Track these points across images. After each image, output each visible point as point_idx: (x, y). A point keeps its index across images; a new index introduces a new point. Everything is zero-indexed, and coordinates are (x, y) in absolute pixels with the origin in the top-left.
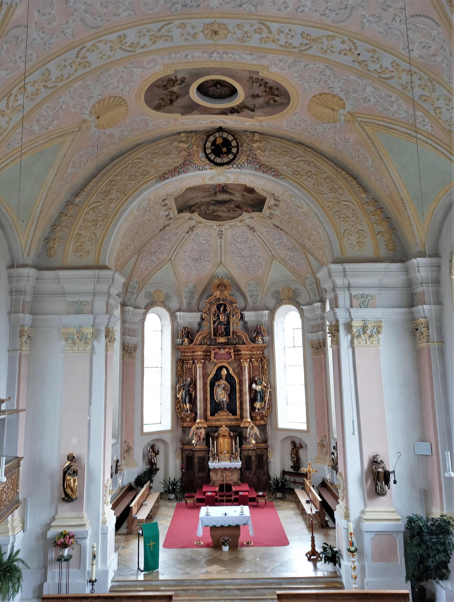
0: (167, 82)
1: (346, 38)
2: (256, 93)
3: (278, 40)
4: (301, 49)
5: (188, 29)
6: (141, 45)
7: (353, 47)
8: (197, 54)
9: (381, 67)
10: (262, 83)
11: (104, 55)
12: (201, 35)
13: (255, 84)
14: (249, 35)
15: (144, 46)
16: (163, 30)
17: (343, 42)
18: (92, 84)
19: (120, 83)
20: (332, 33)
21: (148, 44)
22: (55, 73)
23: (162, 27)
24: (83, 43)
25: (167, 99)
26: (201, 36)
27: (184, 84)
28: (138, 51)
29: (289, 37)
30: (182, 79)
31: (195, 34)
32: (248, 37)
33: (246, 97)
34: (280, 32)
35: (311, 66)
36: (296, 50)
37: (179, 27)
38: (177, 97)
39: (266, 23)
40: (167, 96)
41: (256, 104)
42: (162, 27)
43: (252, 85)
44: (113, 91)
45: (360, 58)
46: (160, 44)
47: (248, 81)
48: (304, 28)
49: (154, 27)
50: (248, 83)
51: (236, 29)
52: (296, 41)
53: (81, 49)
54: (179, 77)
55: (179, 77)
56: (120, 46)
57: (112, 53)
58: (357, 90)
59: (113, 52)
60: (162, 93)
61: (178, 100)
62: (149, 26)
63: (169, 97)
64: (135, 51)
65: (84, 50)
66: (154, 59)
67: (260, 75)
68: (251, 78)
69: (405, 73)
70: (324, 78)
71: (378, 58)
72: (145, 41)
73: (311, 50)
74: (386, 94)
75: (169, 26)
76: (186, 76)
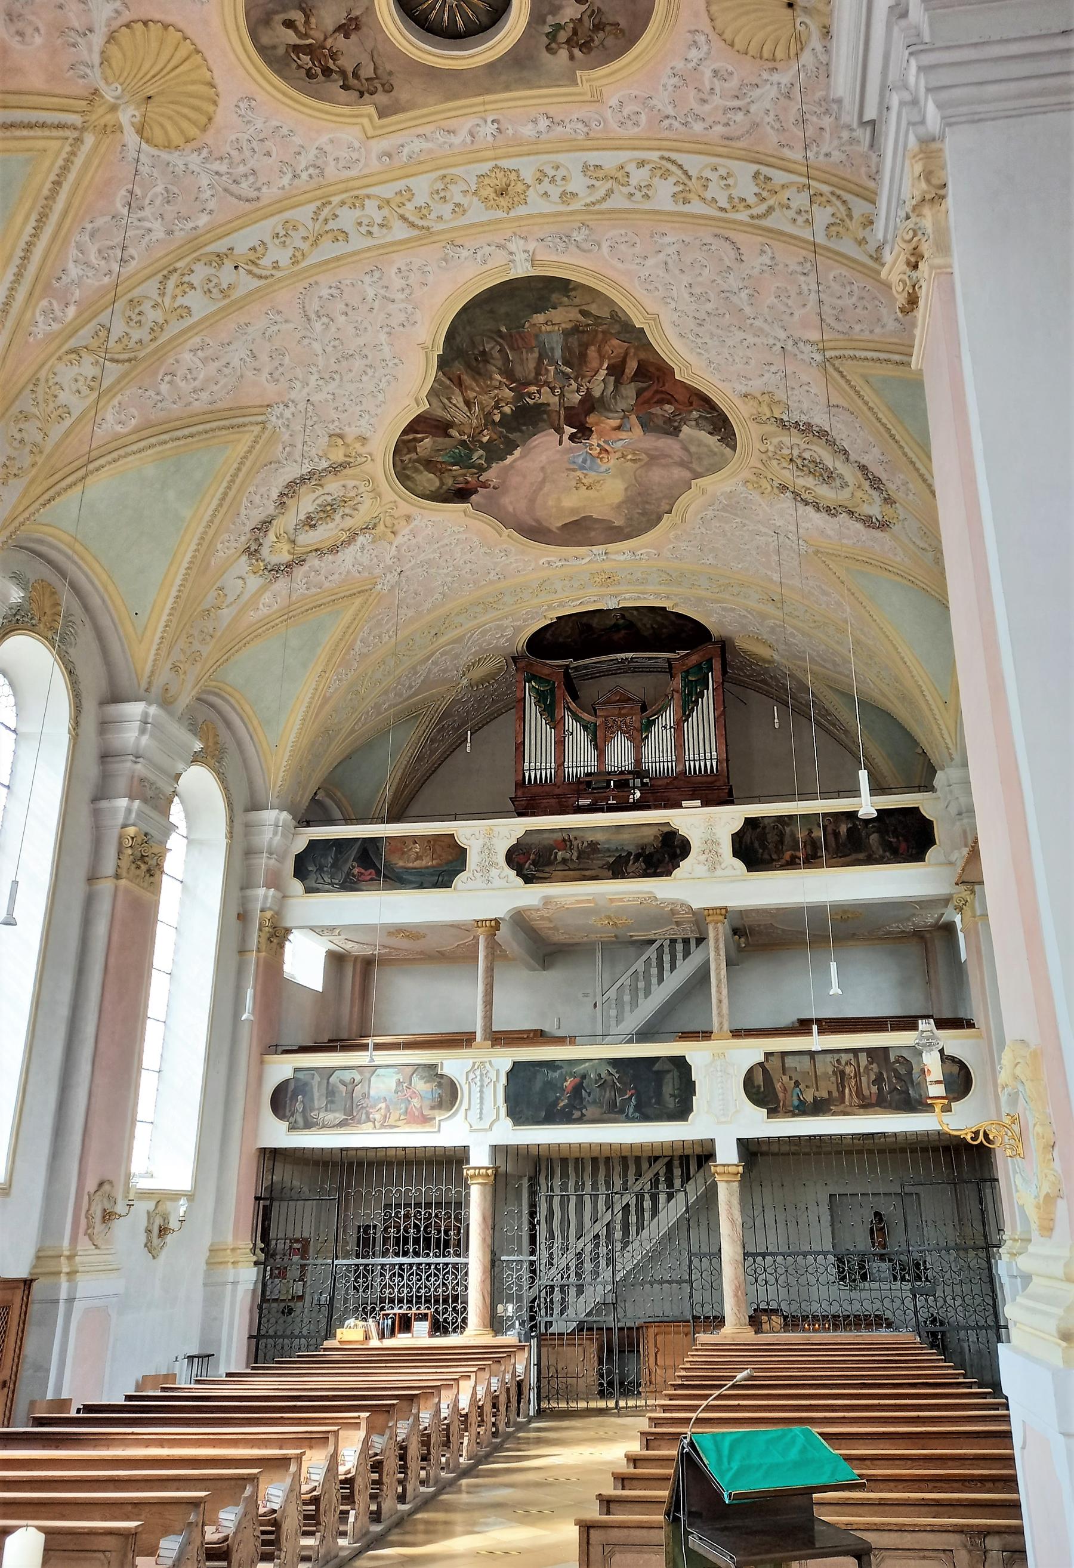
1: (278, 274)
3: (380, 208)
4: (329, 207)
5: (555, 191)
6: (648, 167)
8: (528, 131)
12: (529, 181)
14: (435, 196)
15: (641, 164)
16: (602, 192)
17: (276, 266)
20: (303, 264)
21: (634, 165)
23: (604, 199)
24: (751, 225)
26: (528, 175)
28: (654, 156)
29: (365, 222)
31: (540, 181)
32: (437, 192)
35: (286, 180)
36: (336, 200)
37: (574, 195)
39: (415, 232)
42: (604, 199)
45: (229, 265)
46: (609, 160)
47: (390, 73)
48: (349, 248)
49: (618, 202)
51: (464, 201)
52: (347, 218)
53: (759, 217)
54: (563, 53)
55: (563, 53)
57: (708, 173)
58: (168, 202)
64: (662, 158)
68: (389, 89)
69: (161, 321)
71: (210, 291)
72: (639, 176)
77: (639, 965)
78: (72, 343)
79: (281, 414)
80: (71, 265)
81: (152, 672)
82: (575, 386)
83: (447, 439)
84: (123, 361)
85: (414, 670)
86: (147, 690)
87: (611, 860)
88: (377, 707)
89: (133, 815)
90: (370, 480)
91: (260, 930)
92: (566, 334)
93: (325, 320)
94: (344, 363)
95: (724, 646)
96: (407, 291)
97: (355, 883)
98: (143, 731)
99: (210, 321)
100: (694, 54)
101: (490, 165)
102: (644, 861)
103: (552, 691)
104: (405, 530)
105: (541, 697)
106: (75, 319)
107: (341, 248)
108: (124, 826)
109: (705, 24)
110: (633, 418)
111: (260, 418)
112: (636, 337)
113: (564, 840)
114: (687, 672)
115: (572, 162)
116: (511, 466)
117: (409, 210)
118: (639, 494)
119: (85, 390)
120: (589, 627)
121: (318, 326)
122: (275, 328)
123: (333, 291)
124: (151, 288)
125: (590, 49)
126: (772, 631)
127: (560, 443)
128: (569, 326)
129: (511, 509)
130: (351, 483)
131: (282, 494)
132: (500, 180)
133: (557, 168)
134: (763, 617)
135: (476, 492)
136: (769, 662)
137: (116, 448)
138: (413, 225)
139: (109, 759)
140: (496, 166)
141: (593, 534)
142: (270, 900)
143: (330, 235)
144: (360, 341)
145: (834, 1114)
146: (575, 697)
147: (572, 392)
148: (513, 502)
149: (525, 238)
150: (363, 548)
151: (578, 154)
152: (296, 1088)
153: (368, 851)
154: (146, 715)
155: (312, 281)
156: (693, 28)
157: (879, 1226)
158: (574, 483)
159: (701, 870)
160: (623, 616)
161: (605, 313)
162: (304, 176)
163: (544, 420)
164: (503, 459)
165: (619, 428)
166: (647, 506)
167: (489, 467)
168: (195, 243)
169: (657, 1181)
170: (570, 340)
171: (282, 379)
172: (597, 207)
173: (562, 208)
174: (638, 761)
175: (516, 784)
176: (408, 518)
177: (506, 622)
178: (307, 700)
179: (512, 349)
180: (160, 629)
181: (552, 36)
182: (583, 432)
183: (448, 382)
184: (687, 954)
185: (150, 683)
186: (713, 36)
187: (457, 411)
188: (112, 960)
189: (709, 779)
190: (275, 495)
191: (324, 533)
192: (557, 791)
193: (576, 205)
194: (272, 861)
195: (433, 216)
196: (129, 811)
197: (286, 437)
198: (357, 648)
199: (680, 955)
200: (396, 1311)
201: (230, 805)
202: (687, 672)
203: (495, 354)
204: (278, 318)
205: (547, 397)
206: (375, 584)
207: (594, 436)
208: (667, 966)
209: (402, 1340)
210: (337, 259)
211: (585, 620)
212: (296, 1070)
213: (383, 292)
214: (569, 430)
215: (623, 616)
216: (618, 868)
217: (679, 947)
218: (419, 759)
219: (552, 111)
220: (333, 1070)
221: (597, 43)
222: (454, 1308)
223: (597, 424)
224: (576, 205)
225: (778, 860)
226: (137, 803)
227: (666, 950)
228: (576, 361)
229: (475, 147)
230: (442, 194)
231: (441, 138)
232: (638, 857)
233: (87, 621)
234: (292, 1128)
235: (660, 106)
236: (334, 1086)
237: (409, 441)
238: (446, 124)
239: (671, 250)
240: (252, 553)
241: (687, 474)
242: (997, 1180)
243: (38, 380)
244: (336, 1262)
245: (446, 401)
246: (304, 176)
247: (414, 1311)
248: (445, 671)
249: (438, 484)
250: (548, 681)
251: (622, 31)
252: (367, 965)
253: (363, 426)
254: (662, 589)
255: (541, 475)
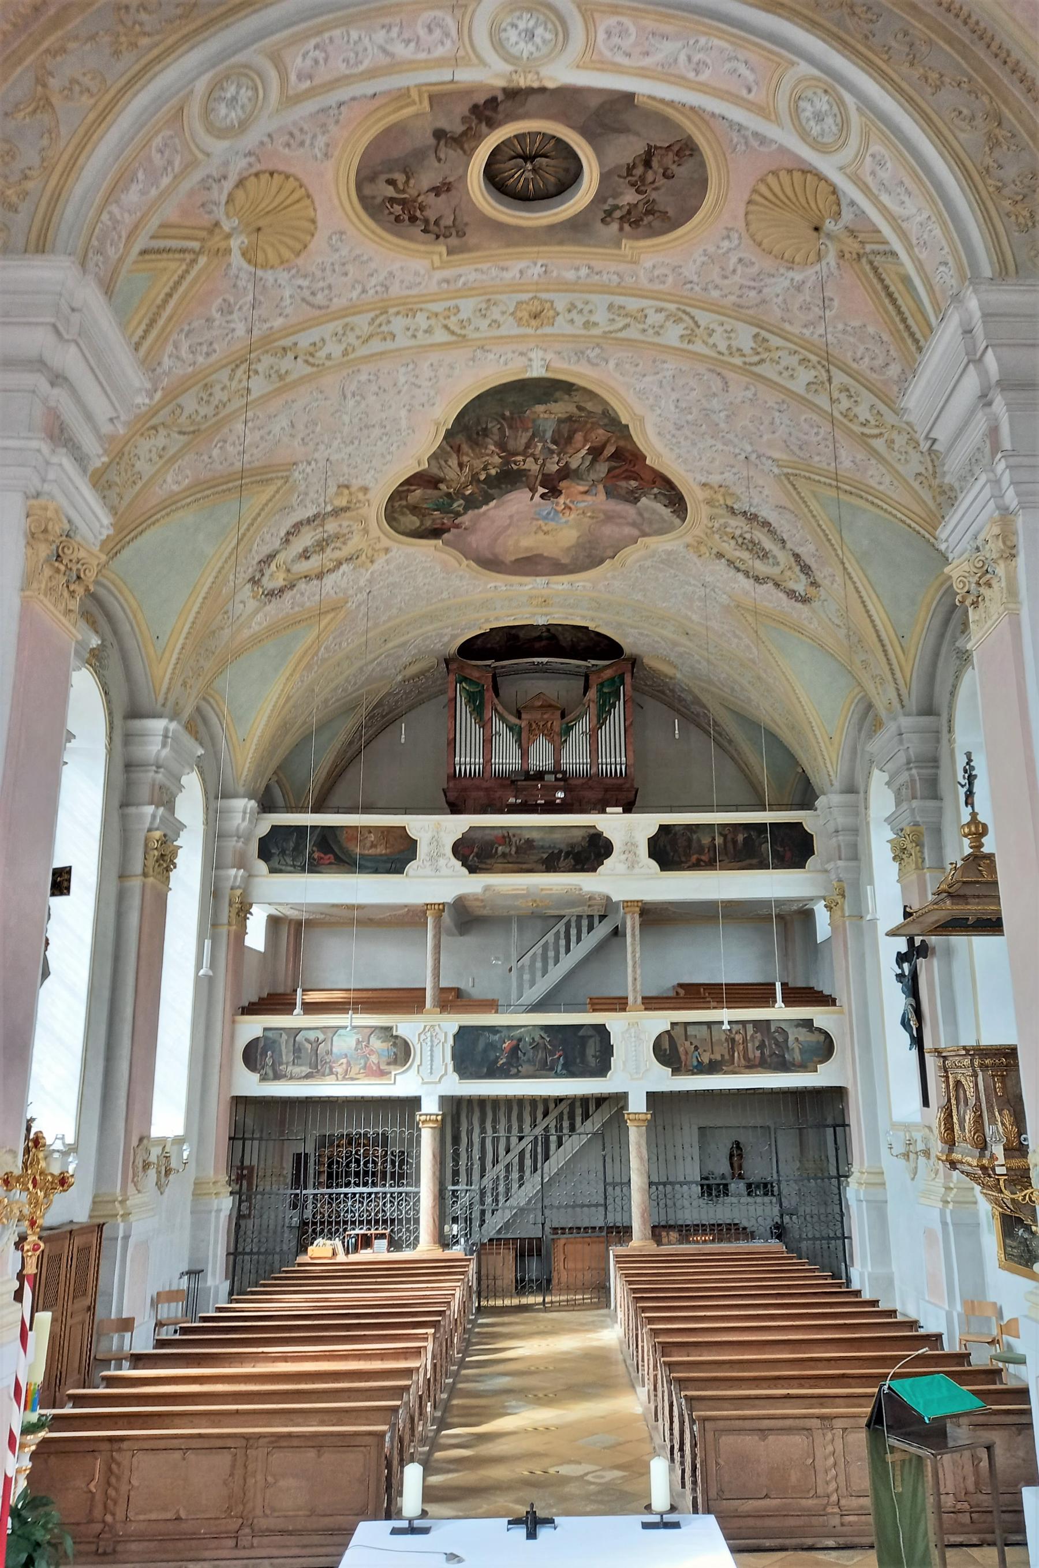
0: (642, 220)
2: (443, 197)
5: (579, 320)
7: (311, 360)
8: (570, 275)
9: (256, 372)
10: (435, 229)
11: (726, 331)
13: (450, 222)
16: (620, 325)
18: (775, 307)
19: (731, 268)
22: (805, 375)
23: (621, 330)
25: (655, 173)
26: (561, 305)
27: (607, 207)
29: (413, 328)
30: (608, 219)
31: (569, 311)
33: (463, 178)
34: (428, 331)
37: (595, 324)
38: (630, 169)
39: (454, 338)
40: (653, 182)
41: (436, 164)
42: (621, 330)
43: (455, 219)
44: (753, 260)
49: (633, 333)
50: (466, 219)
51: (501, 319)
52: (398, 324)
54: (615, 226)
55: (615, 226)
56: (697, 331)
59: (711, 326)
60: (662, 198)
61: (630, 161)
62: (641, 337)
63: (650, 176)
65: (747, 360)
66: (651, 281)
67: (443, 249)
70: (321, 284)
73: (369, 320)
74: (215, 351)
75: (611, 328)
76: (599, 225)
77: (550, 937)
78: (154, 421)
79: (303, 471)
80: (166, 359)
81: (169, 689)
82: (556, 459)
83: (436, 492)
84: (189, 433)
85: (361, 669)
86: (164, 705)
87: (545, 856)
88: (326, 701)
89: (158, 820)
90: (363, 520)
91: (230, 905)
92: (560, 421)
93: (358, 398)
94: (365, 432)
95: (634, 661)
96: (434, 380)
97: (315, 866)
98: (164, 745)
99: (265, 398)
100: (726, 244)
101: (531, 295)
102: (573, 858)
103: (481, 693)
104: (381, 560)
105: (471, 698)
106: (159, 402)
107: (389, 345)
108: (150, 830)
109: (741, 224)
110: (601, 487)
111: (285, 474)
112: (623, 431)
113: (504, 837)
114: (602, 685)
115: (600, 301)
116: (484, 513)
117: (453, 323)
118: (589, 542)
119: (155, 458)
120: (516, 637)
121: (351, 403)
122: (315, 405)
123: (372, 377)
124: (224, 374)
125: (638, 226)
126: (681, 655)
127: (532, 499)
128: (564, 416)
129: (474, 545)
130: (345, 524)
131: (288, 533)
132: (536, 307)
133: (587, 303)
134: (675, 644)
135: (448, 530)
136: (671, 678)
137: (171, 504)
138: (453, 333)
139: (133, 769)
140: (536, 297)
141: (539, 567)
142: (239, 879)
143: (380, 336)
144: (384, 415)
145: (725, 1073)
146: (497, 695)
147: (553, 463)
148: (477, 540)
149: (545, 350)
150: (344, 574)
151: (606, 296)
152: (265, 1045)
153: (327, 837)
154: (166, 730)
155: (355, 369)
156: (730, 226)
157: (737, 1152)
158: (534, 529)
159: (621, 868)
160: (548, 630)
161: (598, 409)
162: (371, 292)
163: (522, 482)
164: (479, 507)
165: (586, 492)
166: (594, 551)
167: (465, 513)
168: (267, 342)
169: (562, 1120)
170: (562, 425)
171: (311, 444)
172: (613, 335)
173: (583, 332)
174: (557, 762)
175: (448, 777)
176: (387, 550)
177: (446, 631)
178: (274, 699)
179: (510, 427)
180: (177, 651)
181: (609, 213)
182: (553, 492)
183: (449, 449)
184: (591, 928)
185: (166, 699)
186: (744, 233)
187: (451, 471)
188: (143, 950)
189: (615, 781)
190: (282, 533)
191: (314, 563)
192: (485, 785)
193: (595, 331)
194: (240, 844)
195: (472, 327)
196: (154, 816)
197: (302, 488)
198: (320, 654)
199: (585, 929)
200: (357, 1231)
201: (206, 793)
202: (602, 685)
203: (495, 430)
204: (320, 396)
205: (531, 466)
206: (347, 602)
207: (563, 496)
208: (573, 939)
209: (365, 1255)
210: (382, 353)
211: (514, 631)
212: (265, 1029)
213: (413, 380)
214: (541, 490)
215: (548, 630)
216: (551, 863)
217: (585, 923)
218: (351, 743)
219: (593, 263)
220: (300, 1030)
221: (645, 222)
222: (408, 1230)
223: (567, 488)
224: (595, 331)
225: (686, 863)
226: (161, 810)
227: (573, 924)
228: (562, 441)
229: (521, 281)
230: (483, 312)
231: (494, 272)
232: (568, 854)
233: (115, 643)
234: (264, 1079)
235: (687, 274)
236: (299, 1044)
237: (403, 491)
238: (502, 264)
239: (670, 373)
240: (254, 581)
241: (635, 532)
242: (849, 1125)
243: (123, 454)
244: (304, 1192)
245: (443, 463)
246: (371, 292)
247: (373, 1231)
248: (386, 670)
249: (418, 524)
250: (477, 684)
251: (669, 218)
252: (298, 925)
253: (368, 480)
254: (590, 613)
255: (508, 521)
